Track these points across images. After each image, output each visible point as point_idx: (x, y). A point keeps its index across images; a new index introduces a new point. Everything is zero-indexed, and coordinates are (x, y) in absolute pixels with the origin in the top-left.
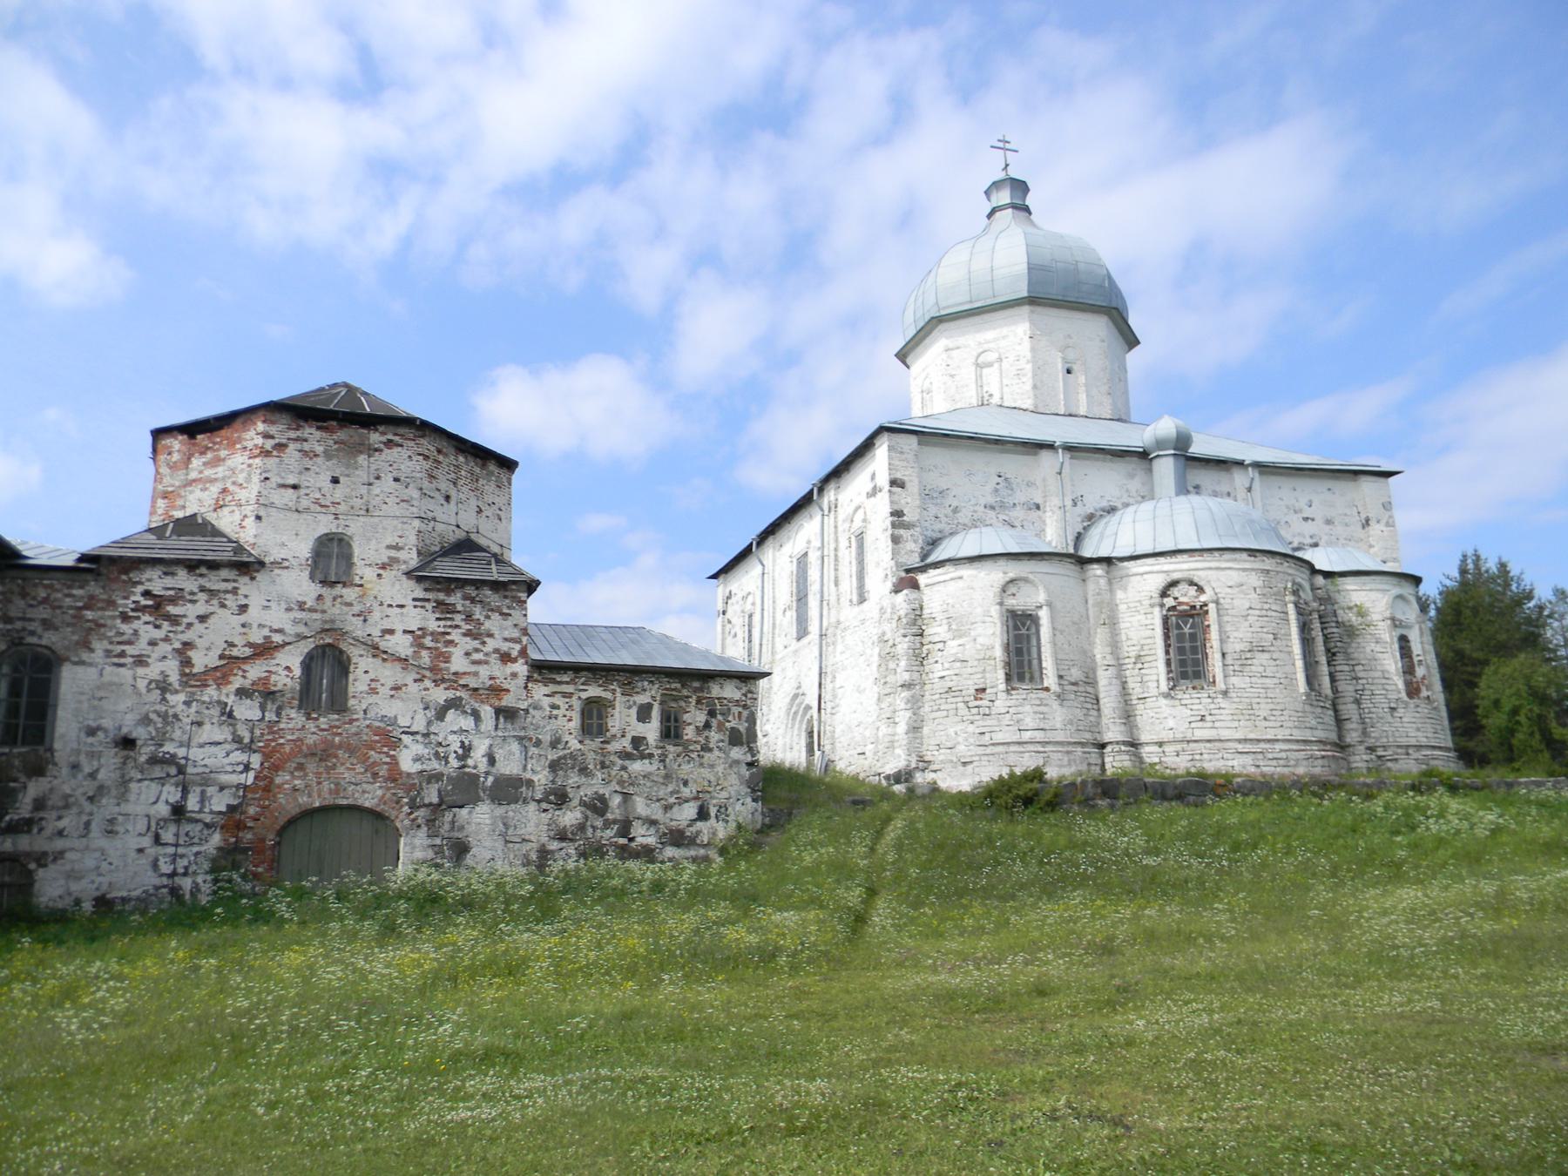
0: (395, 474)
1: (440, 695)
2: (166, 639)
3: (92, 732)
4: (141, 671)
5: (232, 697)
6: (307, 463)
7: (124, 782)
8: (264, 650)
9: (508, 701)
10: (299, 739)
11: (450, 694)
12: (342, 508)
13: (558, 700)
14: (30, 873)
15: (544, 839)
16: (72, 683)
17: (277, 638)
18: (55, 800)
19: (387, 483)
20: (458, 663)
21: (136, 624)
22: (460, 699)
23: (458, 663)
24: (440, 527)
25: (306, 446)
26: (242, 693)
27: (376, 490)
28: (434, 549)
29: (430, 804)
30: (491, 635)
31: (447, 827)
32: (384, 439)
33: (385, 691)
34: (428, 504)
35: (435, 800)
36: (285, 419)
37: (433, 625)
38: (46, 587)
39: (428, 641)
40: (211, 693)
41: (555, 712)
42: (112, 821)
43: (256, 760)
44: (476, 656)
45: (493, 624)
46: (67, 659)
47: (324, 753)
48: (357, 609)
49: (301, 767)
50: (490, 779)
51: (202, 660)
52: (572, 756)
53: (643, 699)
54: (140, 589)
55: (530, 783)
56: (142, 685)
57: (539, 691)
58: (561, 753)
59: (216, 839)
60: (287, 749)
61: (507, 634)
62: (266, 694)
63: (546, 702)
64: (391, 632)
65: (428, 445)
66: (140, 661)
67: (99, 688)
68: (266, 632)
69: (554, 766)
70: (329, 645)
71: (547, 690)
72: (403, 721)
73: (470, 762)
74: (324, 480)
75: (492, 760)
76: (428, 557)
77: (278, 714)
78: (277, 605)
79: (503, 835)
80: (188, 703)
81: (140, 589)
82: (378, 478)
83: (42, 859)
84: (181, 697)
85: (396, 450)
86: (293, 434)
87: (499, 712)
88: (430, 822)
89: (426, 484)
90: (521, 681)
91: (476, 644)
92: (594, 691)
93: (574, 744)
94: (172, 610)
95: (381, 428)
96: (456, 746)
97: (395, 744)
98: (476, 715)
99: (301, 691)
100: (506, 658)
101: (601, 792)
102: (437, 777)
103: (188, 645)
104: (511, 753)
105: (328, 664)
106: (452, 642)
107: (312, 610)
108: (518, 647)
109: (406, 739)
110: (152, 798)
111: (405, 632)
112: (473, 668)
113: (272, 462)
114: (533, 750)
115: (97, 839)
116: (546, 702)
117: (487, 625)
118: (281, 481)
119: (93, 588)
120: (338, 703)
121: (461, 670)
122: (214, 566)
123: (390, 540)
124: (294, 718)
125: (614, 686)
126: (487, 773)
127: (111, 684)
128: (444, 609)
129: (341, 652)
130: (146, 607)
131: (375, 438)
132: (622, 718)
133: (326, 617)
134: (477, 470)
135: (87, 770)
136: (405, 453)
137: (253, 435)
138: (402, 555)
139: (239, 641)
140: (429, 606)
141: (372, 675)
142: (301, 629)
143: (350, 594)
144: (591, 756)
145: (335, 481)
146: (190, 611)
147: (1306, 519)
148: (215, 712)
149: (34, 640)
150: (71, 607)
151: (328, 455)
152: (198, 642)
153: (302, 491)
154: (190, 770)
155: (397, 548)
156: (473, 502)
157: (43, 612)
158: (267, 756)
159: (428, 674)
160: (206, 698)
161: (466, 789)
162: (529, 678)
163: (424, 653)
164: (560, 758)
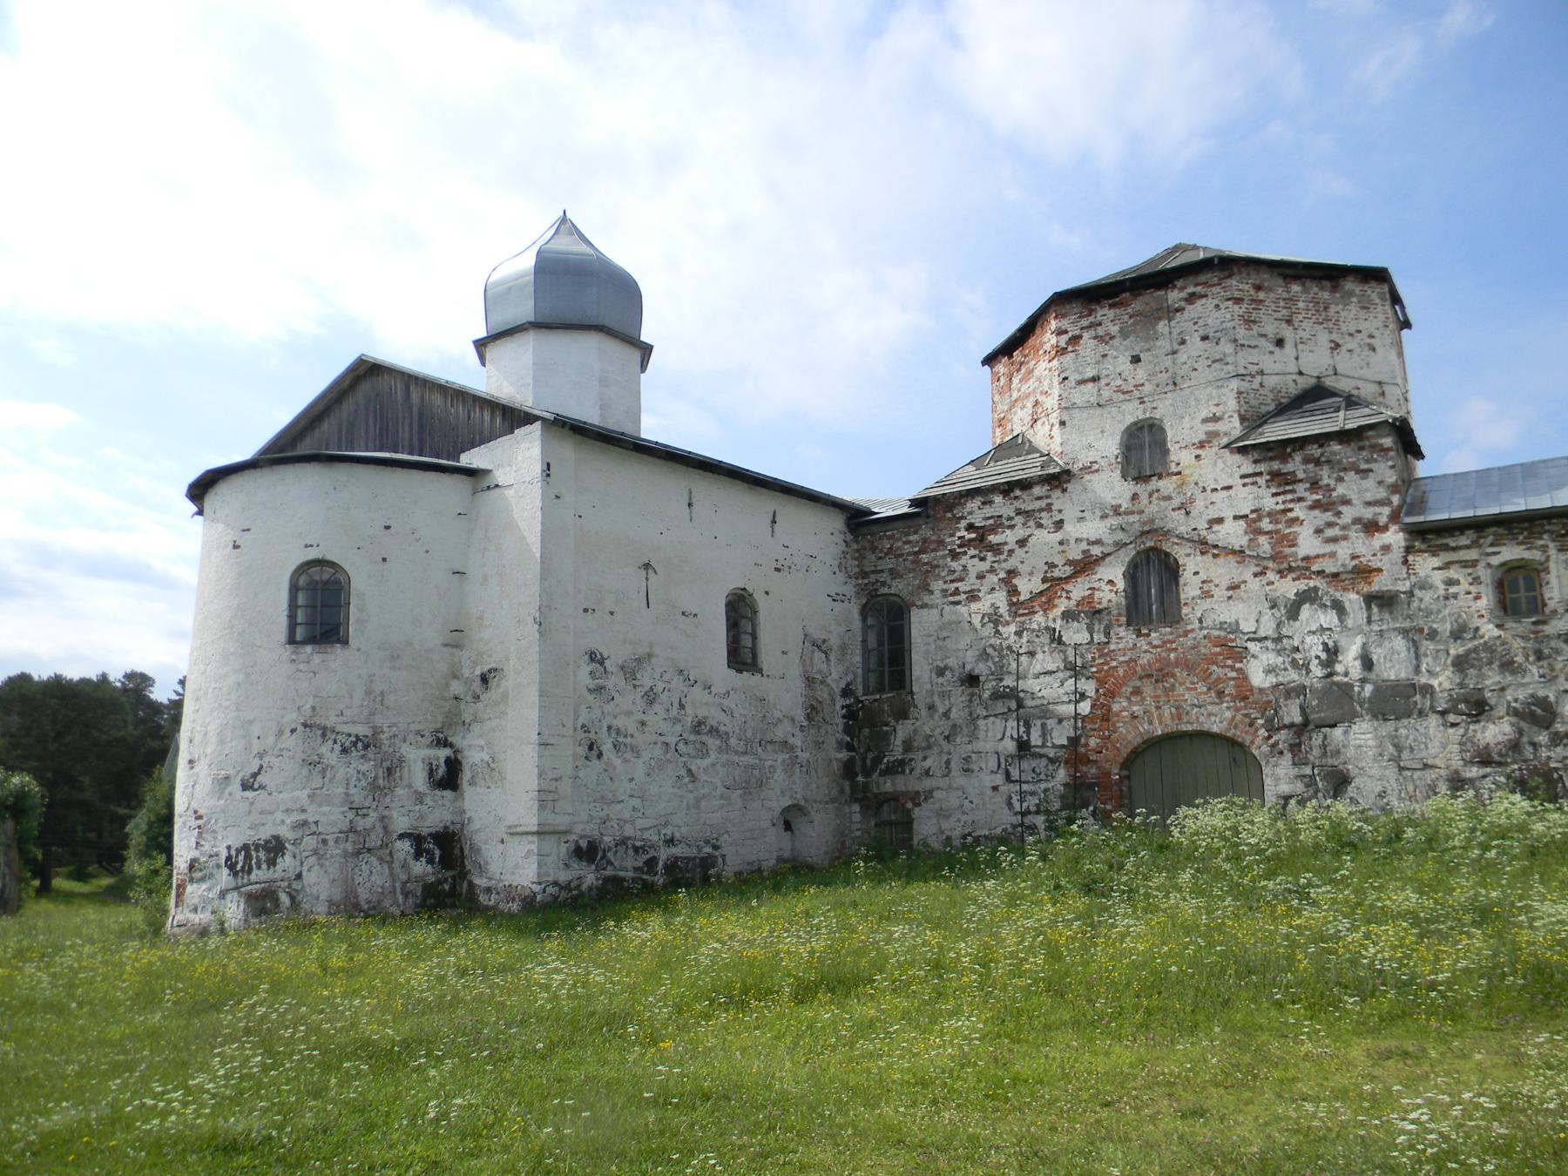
0: (1201, 332)
1: (1289, 588)
2: (992, 571)
3: (941, 672)
4: (974, 606)
5: (1059, 622)
6: (1103, 348)
7: (973, 719)
8: (1085, 565)
9: (1380, 584)
10: (1131, 660)
11: (1302, 585)
12: (1148, 388)
13: (1453, 573)
14: (908, 812)
15: (1457, 763)
16: (921, 624)
17: (1096, 551)
18: (919, 741)
19: (1195, 346)
20: (1308, 544)
21: (964, 560)
22: (1316, 589)
23: (1308, 544)
24: (1270, 381)
25: (1101, 331)
26: (1068, 616)
27: (1182, 357)
28: (1264, 409)
29: (1292, 725)
30: (1346, 502)
31: (1316, 752)
32: (1184, 295)
33: (1220, 593)
34: (1244, 359)
35: (1298, 719)
36: (1076, 307)
37: (1269, 503)
38: (889, 538)
39: (1266, 524)
40: (1039, 619)
41: (1452, 590)
42: (967, 759)
43: (1089, 687)
44: (1330, 533)
46: (913, 604)
47: (1160, 674)
48: (1176, 502)
49: (1137, 691)
50: (1369, 688)
51: (1028, 586)
52: (1487, 647)
54: (963, 523)
55: (1428, 690)
56: (976, 620)
57: (1426, 565)
58: (1470, 645)
59: (1062, 774)
60: (1121, 671)
61: (1369, 497)
62: (1092, 613)
63: (1438, 578)
64: (1220, 521)
65: (1239, 285)
66: (973, 596)
67: (941, 628)
68: (1084, 546)
69: (1460, 664)
70: (1151, 549)
71: (1436, 562)
72: (1247, 626)
73: (1339, 668)
74: (1123, 363)
75: (1367, 663)
76: (1253, 420)
77: (1107, 634)
78: (1093, 515)
79: (1396, 759)
80: (1019, 634)
81: (963, 523)
82: (1183, 342)
83: (917, 798)
84: (1013, 628)
85: (1199, 303)
86: (1085, 322)
87: (1370, 599)
88: (1295, 748)
89: (1241, 333)
90: (1397, 554)
91: (1329, 516)
92: (1511, 552)
93: (1489, 630)
94: (993, 539)
95: (1179, 283)
96: (1318, 650)
97: (1241, 654)
98: (1339, 607)
99: (1128, 607)
101: (1541, 693)
102: (1301, 690)
103: (1012, 573)
104: (1393, 651)
105: (1154, 574)
106: (1297, 519)
107: (1129, 513)
108: (1386, 511)
109: (1253, 647)
110: (998, 736)
111: (1236, 518)
112: (1328, 548)
113: (1069, 357)
114: (1428, 646)
116: (1438, 578)
117: (1340, 490)
118: (1078, 377)
119: (926, 531)
120: (1170, 613)
121: (1313, 553)
122: (1025, 485)
123: (1204, 414)
124: (1124, 637)
125: (1545, 540)
126: (1363, 681)
127: (950, 623)
128: (1282, 481)
129: (1167, 554)
130: (970, 540)
131: (1174, 296)
133: (1145, 517)
134: (1326, 295)
135: (941, 710)
136: (1209, 303)
137: (1048, 338)
138: (1221, 427)
139: (1059, 561)
140: (1261, 481)
141: (1203, 576)
142: (1120, 536)
143: (1167, 485)
144: (1517, 644)
145: (1136, 360)
146: (1009, 537)
148: (1045, 639)
149: (885, 590)
150: (909, 554)
151: (1124, 334)
152: (1022, 568)
153: (1103, 382)
154: (1029, 703)
155: (1215, 419)
156: (1324, 338)
157: (888, 563)
158: (1101, 682)
159: (1271, 564)
160: (1035, 626)
161: (1338, 703)
162: (1409, 550)
163: (1263, 540)
164: (1468, 652)
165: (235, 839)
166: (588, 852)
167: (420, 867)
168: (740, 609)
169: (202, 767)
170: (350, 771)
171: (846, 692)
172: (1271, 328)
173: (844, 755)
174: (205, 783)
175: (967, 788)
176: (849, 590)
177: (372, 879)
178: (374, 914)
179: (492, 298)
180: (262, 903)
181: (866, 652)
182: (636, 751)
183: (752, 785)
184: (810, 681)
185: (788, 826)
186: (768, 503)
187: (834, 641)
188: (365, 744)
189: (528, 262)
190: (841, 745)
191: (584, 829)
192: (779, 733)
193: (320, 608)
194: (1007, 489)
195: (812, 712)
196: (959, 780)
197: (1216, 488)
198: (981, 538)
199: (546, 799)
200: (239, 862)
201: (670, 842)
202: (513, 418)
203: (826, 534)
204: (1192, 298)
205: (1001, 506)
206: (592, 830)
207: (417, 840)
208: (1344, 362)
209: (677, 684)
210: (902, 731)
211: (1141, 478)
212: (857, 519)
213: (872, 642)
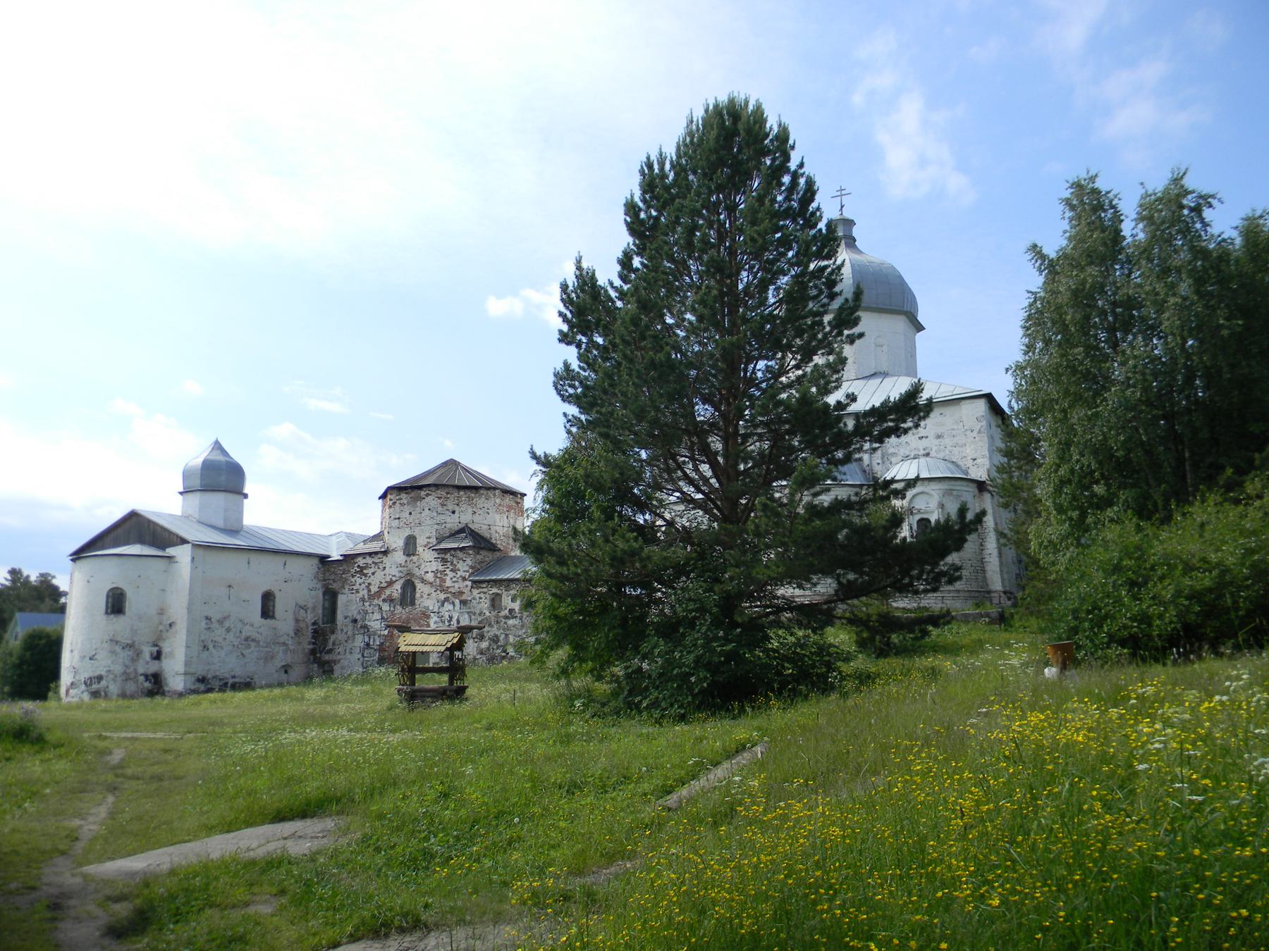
1: (442, 596)
8: (391, 583)
9: (464, 597)
16: (341, 600)
20: (449, 583)
24: (448, 526)
26: (384, 600)
37: (441, 568)
40: (376, 601)
45: (460, 565)
51: (374, 589)
53: (513, 592)
57: (475, 592)
62: (390, 600)
65: (442, 493)
76: (440, 540)
78: (393, 566)
83: (335, 662)
89: (440, 509)
92: (495, 590)
97: (428, 617)
100: (464, 579)
105: (409, 586)
110: (359, 641)
115: (348, 656)
120: (413, 603)
122: (376, 553)
128: (444, 561)
131: (423, 493)
132: (507, 601)
143: (415, 558)
147: (921, 438)
151: (408, 504)
156: (470, 510)
165: (87, 675)
166: (202, 680)
167: (147, 685)
168: (268, 598)
169: (76, 653)
170: (124, 655)
171: (314, 624)
172: (451, 507)
173: (311, 647)
174: (77, 658)
175: (350, 655)
176: (319, 586)
177: (131, 687)
178: (132, 697)
179: (187, 475)
180: (95, 694)
181: (324, 608)
182: (222, 648)
183: (269, 658)
184: (297, 621)
185: (286, 672)
186: (280, 559)
187: (310, 605)
188: (131, 646)
189: (200, 461)
190: (309, 643)
191: (201, 672)
192: (282, 640)
193: (116, 603)
194: (370, 554)
195: (298, 632)
196: (348, 656)
197: (428, 562)
198: (361, 571)
199: (187, 664)
200: (88, 682)
201: (234, 677)
202: (184, 541)
203: (311, 566)
204: (428, 495)
205: (369, 560)
206: (203, 673)
207: (146, 677)
208: (477, 518)
209: (239, 625)
210: (333, 638)
211: (408, 555)
212: (323, 559)
213: (327, 605)
